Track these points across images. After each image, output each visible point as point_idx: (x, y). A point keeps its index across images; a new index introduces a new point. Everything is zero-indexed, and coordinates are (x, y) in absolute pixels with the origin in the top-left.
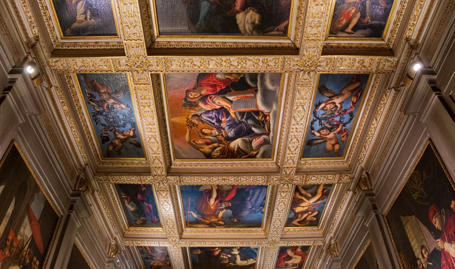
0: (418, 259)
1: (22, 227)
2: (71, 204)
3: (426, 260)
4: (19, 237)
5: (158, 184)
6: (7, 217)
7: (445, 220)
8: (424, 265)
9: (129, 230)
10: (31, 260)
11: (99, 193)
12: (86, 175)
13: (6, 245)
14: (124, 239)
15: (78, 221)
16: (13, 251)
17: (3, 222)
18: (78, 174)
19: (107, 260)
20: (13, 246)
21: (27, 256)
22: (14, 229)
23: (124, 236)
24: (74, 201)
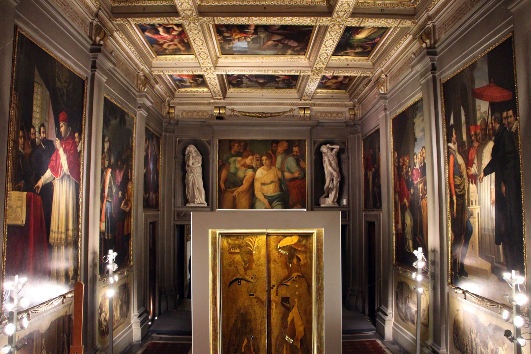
0: (34, 128)
3: (41, 138)
4: (479, 123)
7: (68, 135)
8: (37, 140)
16: (479, 138)
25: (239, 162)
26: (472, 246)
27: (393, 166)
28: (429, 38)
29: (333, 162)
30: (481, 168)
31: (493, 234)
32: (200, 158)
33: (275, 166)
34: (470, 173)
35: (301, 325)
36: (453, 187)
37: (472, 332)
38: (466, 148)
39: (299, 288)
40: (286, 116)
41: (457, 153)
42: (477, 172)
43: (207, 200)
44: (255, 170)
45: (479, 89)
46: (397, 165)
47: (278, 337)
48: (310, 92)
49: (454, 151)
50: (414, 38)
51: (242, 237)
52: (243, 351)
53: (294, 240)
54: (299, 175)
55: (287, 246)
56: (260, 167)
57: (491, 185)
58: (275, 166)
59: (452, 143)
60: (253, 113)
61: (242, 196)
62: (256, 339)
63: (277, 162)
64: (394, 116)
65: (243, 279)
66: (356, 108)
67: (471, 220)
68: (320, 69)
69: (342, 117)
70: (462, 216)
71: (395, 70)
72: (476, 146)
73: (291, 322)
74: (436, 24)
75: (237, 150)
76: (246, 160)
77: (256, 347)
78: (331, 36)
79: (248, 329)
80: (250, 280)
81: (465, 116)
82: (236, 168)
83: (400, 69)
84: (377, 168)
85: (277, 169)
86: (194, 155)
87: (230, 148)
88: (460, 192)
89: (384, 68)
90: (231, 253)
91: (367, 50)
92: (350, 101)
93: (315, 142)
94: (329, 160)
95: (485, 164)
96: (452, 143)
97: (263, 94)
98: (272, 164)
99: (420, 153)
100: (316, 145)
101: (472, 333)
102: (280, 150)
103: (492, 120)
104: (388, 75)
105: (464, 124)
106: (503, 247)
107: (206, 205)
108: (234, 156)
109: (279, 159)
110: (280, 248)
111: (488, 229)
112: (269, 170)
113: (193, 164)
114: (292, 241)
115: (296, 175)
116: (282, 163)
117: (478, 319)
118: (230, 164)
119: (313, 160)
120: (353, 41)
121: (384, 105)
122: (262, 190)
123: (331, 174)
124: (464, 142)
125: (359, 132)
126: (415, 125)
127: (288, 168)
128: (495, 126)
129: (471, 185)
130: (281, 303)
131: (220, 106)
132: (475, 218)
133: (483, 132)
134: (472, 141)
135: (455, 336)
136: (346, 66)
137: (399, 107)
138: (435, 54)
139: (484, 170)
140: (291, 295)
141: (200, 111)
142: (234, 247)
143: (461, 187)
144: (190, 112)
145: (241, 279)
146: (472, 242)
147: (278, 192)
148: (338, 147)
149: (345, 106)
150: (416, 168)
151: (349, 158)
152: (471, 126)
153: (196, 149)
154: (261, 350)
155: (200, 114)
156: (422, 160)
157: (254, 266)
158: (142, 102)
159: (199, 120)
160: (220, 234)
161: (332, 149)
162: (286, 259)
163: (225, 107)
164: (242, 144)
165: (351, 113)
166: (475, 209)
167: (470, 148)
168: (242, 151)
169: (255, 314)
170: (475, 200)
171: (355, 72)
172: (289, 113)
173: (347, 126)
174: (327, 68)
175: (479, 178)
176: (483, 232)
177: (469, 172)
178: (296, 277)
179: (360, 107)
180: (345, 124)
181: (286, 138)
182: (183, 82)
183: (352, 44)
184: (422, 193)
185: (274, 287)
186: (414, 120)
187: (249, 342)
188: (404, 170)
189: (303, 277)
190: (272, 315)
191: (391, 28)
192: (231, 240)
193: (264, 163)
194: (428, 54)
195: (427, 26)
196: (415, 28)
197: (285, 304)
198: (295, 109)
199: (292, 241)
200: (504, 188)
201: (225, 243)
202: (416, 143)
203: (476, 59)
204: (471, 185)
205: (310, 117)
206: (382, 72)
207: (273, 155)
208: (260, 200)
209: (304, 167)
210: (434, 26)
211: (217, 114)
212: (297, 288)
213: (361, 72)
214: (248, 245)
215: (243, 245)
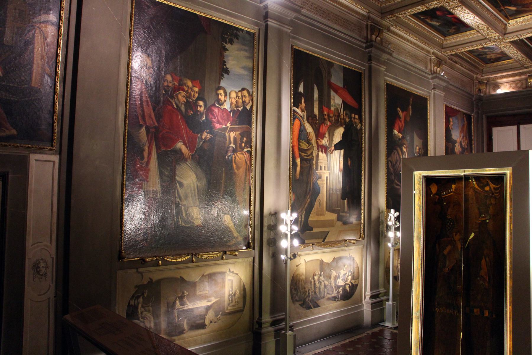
1: (332, 100)
2: (369, 55)
4: (332, 109)
5: (447, 4)
6: (316, 101)
9: (446, 40)
10: (350, 118)
11: (395, 27)
12: (373, 21)
13: (325, 119)
14: (443, 50)
15: (382, 66)
16: (332, 120)
17: (315, 106)
18: (365, 23)
19: (430, 77)
20: (331, 117)
21: (345, 117)
22: (326, 105)
23: (442, 47)
24: (370, 52)
26: (320, 203)
30: (332, 143)
31: (339, 193)
34: (320, 144)
36: (296, 150)
37: (316, 275)
38: (317, 122)
57: (340, 158)
67: (319, 182)
72: (328, 124)
96: (299, 109)
103: (343, 113)
111: (336, 189)
124: (315, 116)
129: (320, 153)
134: (325, 119)
139: (335, 146)
143: (309, 153)
146: (320, 200)
150: (222, 107)
166: (325, 174)
170: (325, 167)
175: (329, 150)
176: (331, 192)
177: (319, 142)
184: (235, 143)
200: (350, 162)
204: (320, 153)
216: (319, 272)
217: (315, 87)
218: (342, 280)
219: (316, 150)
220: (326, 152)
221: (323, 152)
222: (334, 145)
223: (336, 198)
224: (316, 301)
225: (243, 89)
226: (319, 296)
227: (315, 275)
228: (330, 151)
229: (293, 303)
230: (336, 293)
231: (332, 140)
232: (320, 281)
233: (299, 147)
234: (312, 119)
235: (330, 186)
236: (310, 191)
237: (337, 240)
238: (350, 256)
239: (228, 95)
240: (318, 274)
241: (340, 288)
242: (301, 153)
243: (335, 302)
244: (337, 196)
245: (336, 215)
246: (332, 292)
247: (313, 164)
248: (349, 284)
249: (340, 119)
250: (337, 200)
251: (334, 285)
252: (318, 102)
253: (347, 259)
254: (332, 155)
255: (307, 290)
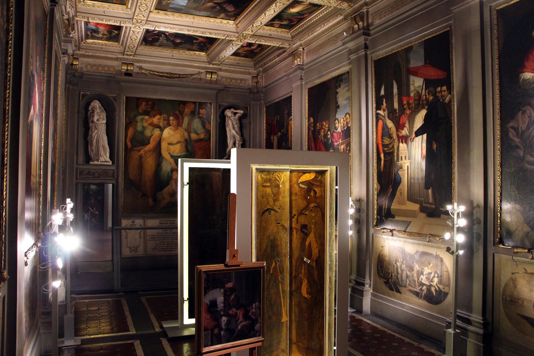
4: (412, 95)
16: (412, 107)
21: (427, 96)
25: (146, 120)
26: (401, 192)
27: (307, 130)
28: (362, 21)
29: (236, 126)
31: (422, 182)
32: (104, 115)
33: (181, 126)
34: (401, 135)
35: (317, 247)
37: (398, 261)
38: (397, 115)
39: (315, 216)
40: (194, 79)
41: (387, 119)
42: (408, 134)
43: (111, 157)
44: (162, 130)
45: (413, 68)
46: (313, 129)
47: (297, 259)
48: (223, 56)
49: (384, 117)
50: (345, 19)
51: (272, 173)
52: (272, 272)
53: (312, 176)
54: (204, 136)
55: (306, 181)
56: (167, 127)
57: (422, 144)
58: (181, 126)
59: (382, 110)
60: (161, 73)
61: (148, 155)
62: (281, 261)
63: (184, 123)
64: (310, 86)
65: (273, 210)
66: (259, 77)
67: (400, 172)
68: (245, 36)
69: (245, 84)
70: (390, 170)
71: (315, 44)
72: (408, 113)
73: (308, 246)
74: (369, 10)
75: (144, 109)
76: (154, 119)
77: (281, 268)
78: (276, 7)
79: (275, 253)
80: (278, 210)
81: (398, 88)
82: (143, 127)
83: (321, 44)
84: (285, 133)
85: (184, 130)
86: (98, 111)
87: (138, 107)
88: (389, 150)
89: (303, 41)
90: (264, 186)
91: (292, 24)
92: (254, 70)
93: (220, 106)
94: (232, 124)
95: (416, 128)
96: (382, 110)
97: (173, 55)
98: (179, 124)
99: (343, 118)
100: (221, 109)
101: (397, 263)
102: (188, 112)
104: (305, 49)
105: (396, 95)
106: (432, 191)
107: (111, 164)
108: (141, 114)
109: (186, 120)
110: (300, 183)
111: (418, 178)
112: (176, 131)
113: (98, 120)
114: (310, 177)
115: (202, 136)
116: (189, 124)
117: (405, 250)
118: (137, 122)
119: (218, 123)
120: (286, 13)
121: (300, 75)
122: (168, 150)
123: (234, 137)
124: (396, 110)
125: (262, 100)
126: (338, 94)
127: (194, 130)
128: (428, 98)
129: (401, 144)
130: (300, 229)
131: (128, 62)
132: (404, 170)
133: (416, 102)
134: (404, 109)
135: (379, 267)
136: (269, 36)
137: (319, 77)
138: (369, 35)
139: (416, 133)
140: (309, 222)
141: (107, 66)
142: (266, 181)
143: (391, 146)
144: (95, 65)
145: (272, 209)
146: (401, 189)
147: (185, 152)
148: (242, 112)
149: (250, 74)
150: (337, 131)
151: (250, 124)
152: (404, 96)
153: (100, 105)
154: (285, 271)
155: (106, 68)
156: (345, 125)
157: (280, 198)
158: (66, 48)
159: (103, 75)
160: (257, 169)
161: (235, 114)
162: (305, 193)
163: (133, 64)
164: (150, 103)
165: (254, 81)
166: (405, 163)
167: (402, 114)
168: (149, 110)
169: (281, 240)
170: (405, 157)
171: (275, 42)
172: (196, 76)
173: (250, 92)
174: (254, 36)
175: (410, 138)
176: (412, 181)
178: (313, 208)
179: (264, 76)
180: (248, 91)
181: (193, 100)
182: (95, 33)
183: (283, 16)
185: (295, 217)
186: (338, 90)
187: (276, 264)
188: (322, 134)
189: (319, 207)
190: (293, 241)
191: (324, 6)
192: (264, 175)
193: (171, 124)
194: (364, 34)
195: (362, 11)
196: (349, 10)
197: (304, 230)
198: (202, 73)
199: (310, 177)
200: (435, 146)
201: (259, 177)
202: (338, 110)
203: (413, 44)
204: (401, 144)
205: (216, 82)
206: (301, 45)
207: (180, 116)
208: (166, 160)
209: (209, 129)
210: (367, 12)
211: (124, 71)
212: (313, 216)
213: (281, 43)
214: (276, 180)
215: (273, 179)
216: (401, 260)
217: (394, 82)
218: (426, 278)
219: (397, 143)
220: (406, 142)
221: (404, 142)
222: (416, 132)
223: (418, 188)
224: (398, 287)
225: (346, 114)
226: (401, 283)
227: (397, 260)
228: (411, 139)
229: (379, 278)
230: (419, 290)
231: (413, 127)
232: (402, 269)
233: (382, 144)
234: (393, 114)
235: (411, 175)
236: (392, 181)
237: (420, 232)
238: (436, 255)
239: (339, 121)
240: (401, 261)
241: (423, 286)
242: (384, 148)
243: (417, 298)
244: (419, 185)
245: (419, 206)
246: (415, 285)
247: (394, 156)
248: (434, 287)
249: (422, 101)
250: (419, 190)
251: (416, 279)
252: (397, 96)
253: (433, 257)
254: (412, 143)
255: (390, 272)
